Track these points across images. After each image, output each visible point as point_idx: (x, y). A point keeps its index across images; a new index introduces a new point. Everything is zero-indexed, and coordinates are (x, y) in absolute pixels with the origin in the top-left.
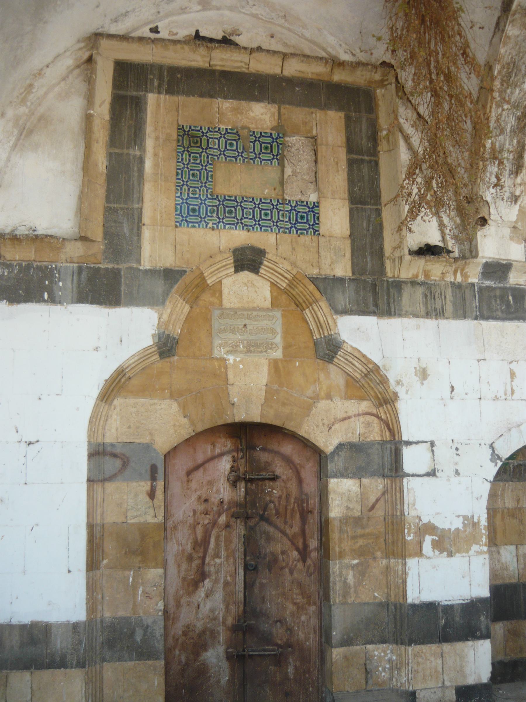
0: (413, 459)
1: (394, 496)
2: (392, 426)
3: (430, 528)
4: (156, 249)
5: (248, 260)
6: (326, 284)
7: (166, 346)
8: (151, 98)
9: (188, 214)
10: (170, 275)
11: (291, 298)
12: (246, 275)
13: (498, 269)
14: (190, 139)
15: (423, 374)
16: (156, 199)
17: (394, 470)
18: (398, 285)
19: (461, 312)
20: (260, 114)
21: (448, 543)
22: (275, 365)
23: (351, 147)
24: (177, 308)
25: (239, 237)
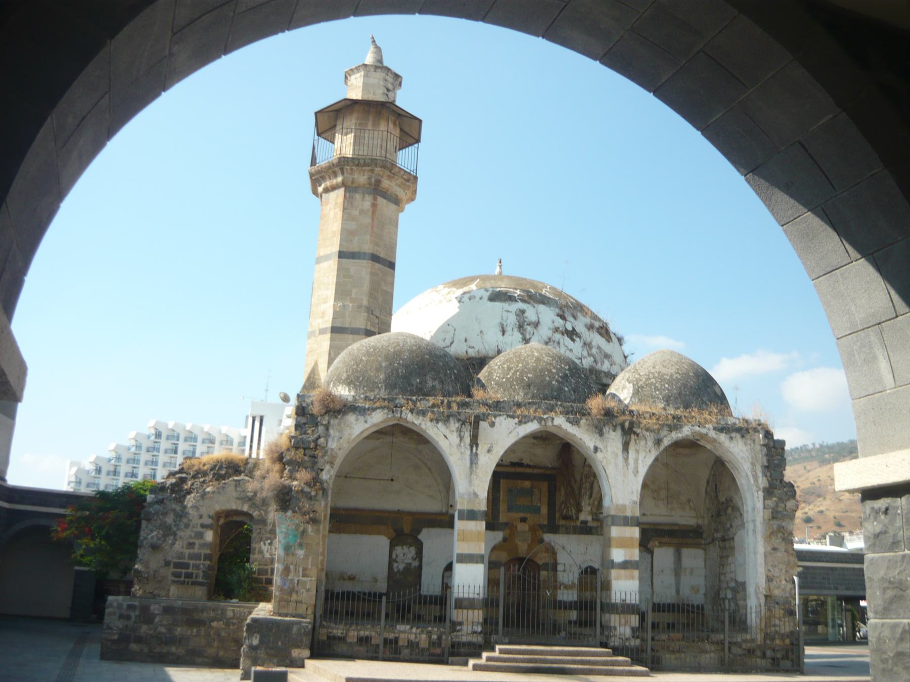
0: (560, 568)
1: (555, 576)
2: (555, 560)
3: (563, 584)
4: (503, 518)
5: (523, 520)
6: (541, 526)
7: (505, 540)
8: (502, 481)
9: (510, 509)
10: (506, 524)
11: (533, 529)
12: (523, 523)
13: (585, 522)
14: (510, 491)
15: (563, 548)
16: (503, 507)
17: (555, 569)
18: (559, 526)
19: (575, 533)
20: (527, 484)
21: (566, 587)
22: (529, 545)
23: (549, 492)
24: (507, 531)
25: (522, 515)
